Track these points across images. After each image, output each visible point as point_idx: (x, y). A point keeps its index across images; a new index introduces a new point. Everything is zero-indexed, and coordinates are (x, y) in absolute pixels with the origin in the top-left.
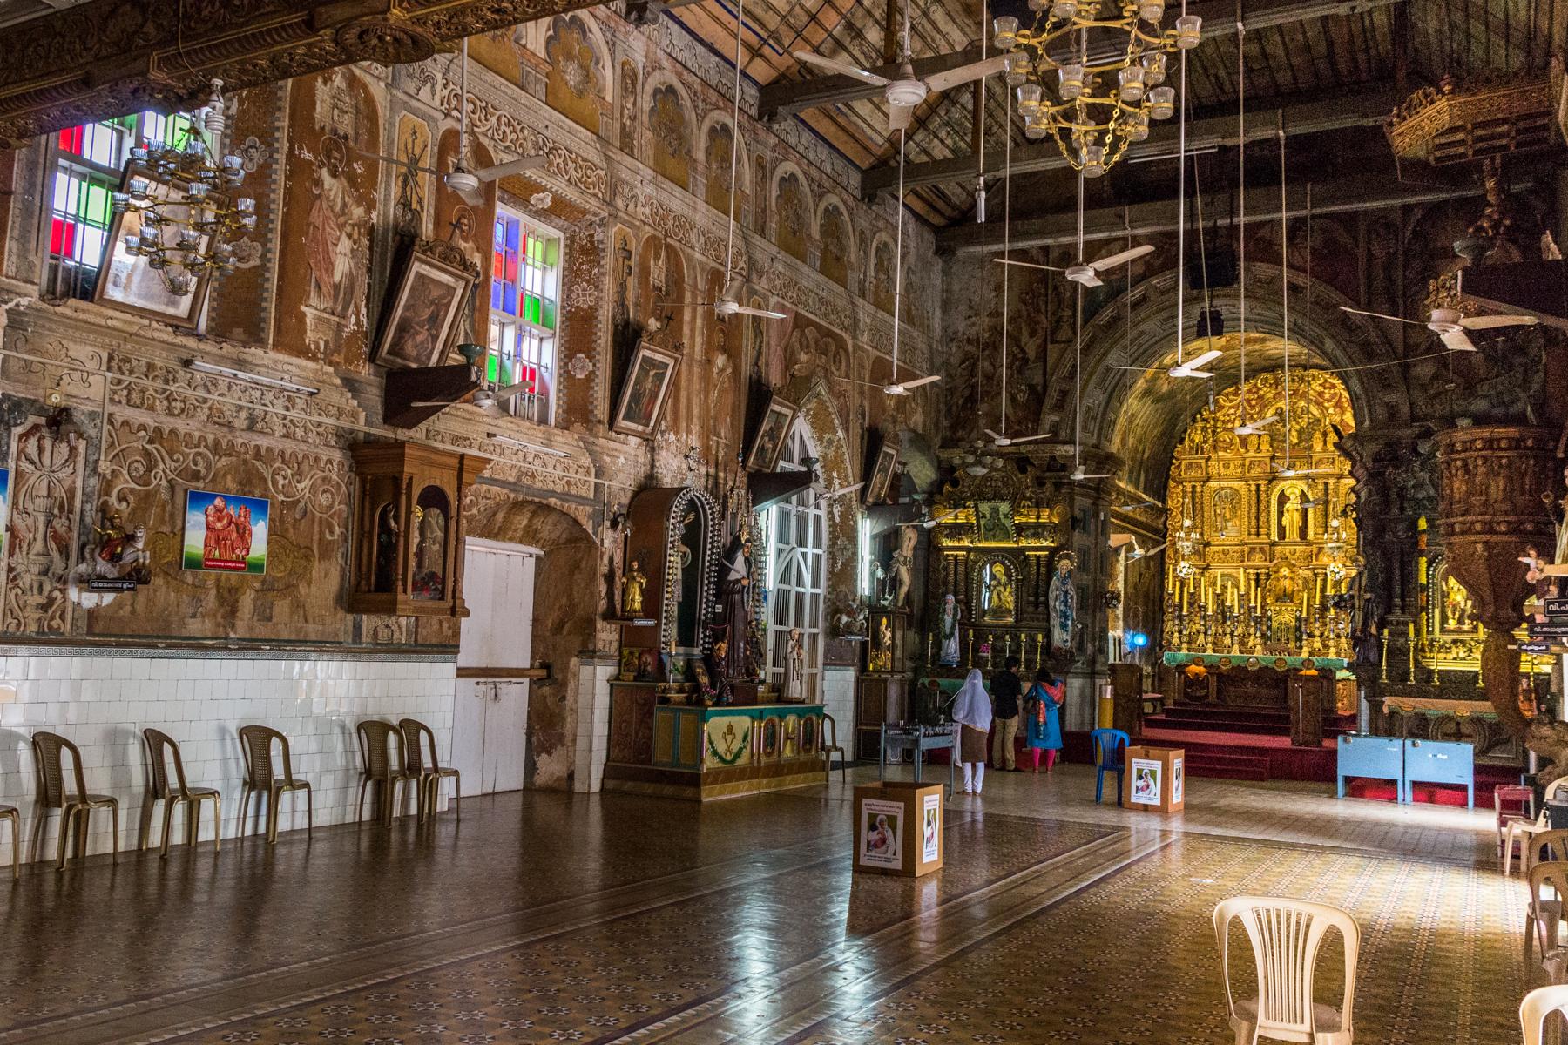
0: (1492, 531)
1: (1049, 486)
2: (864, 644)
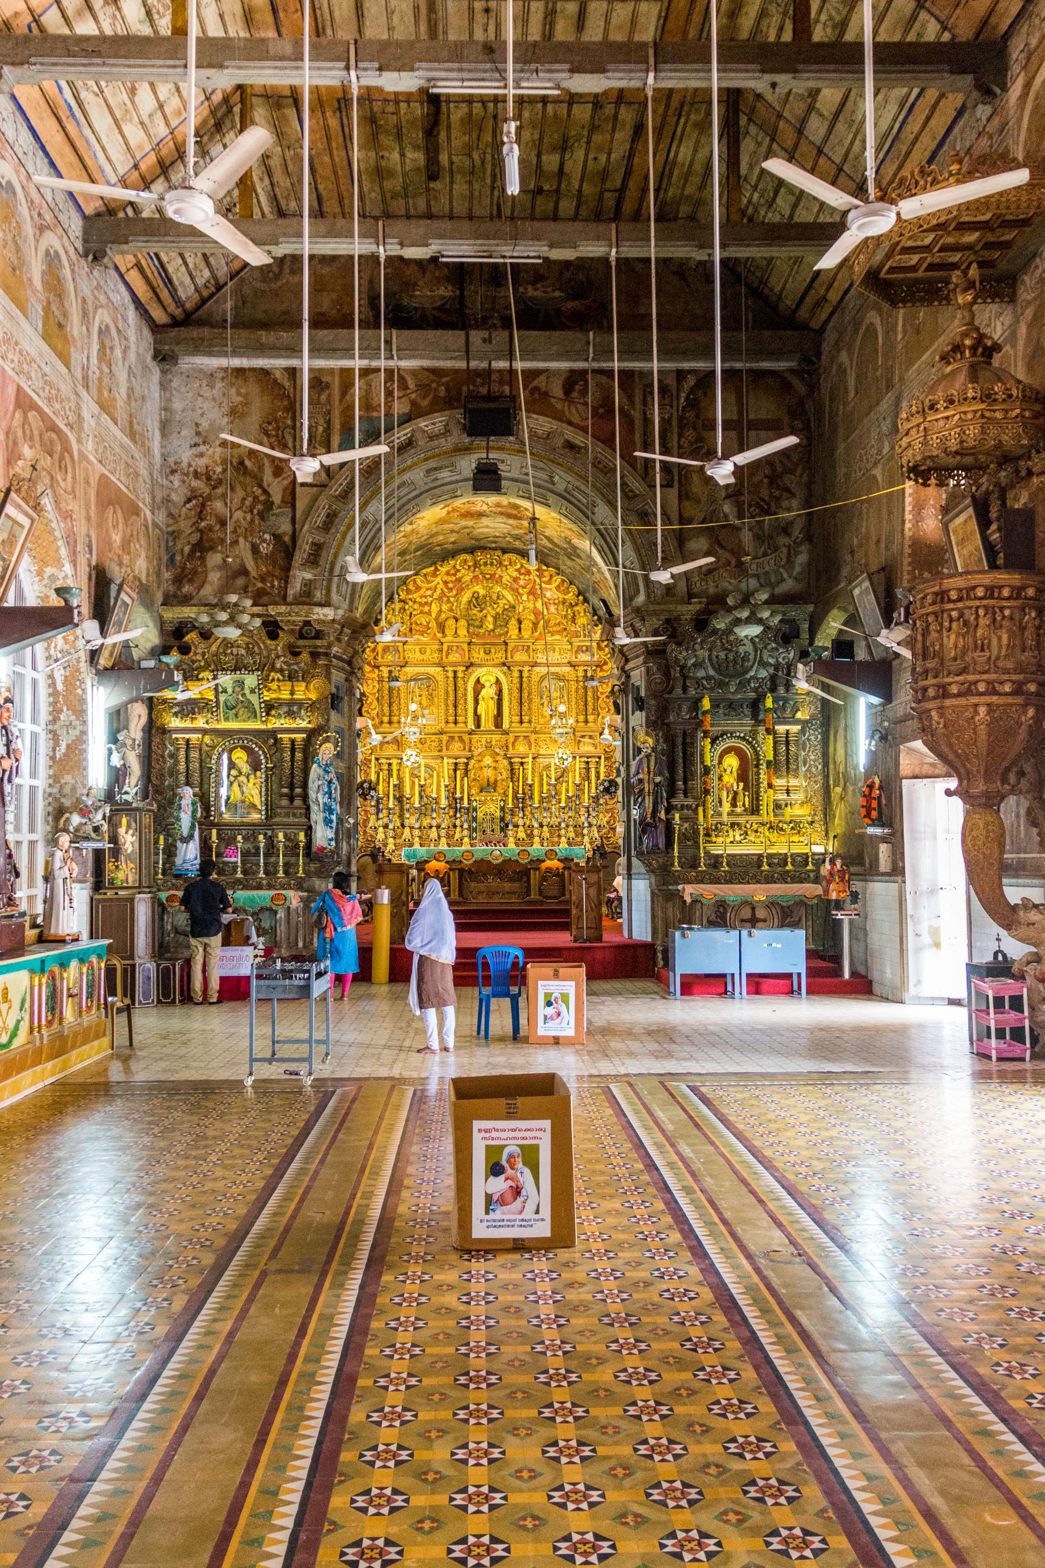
0: (995, 692)
1: (305, 656)
2: (98, 854)
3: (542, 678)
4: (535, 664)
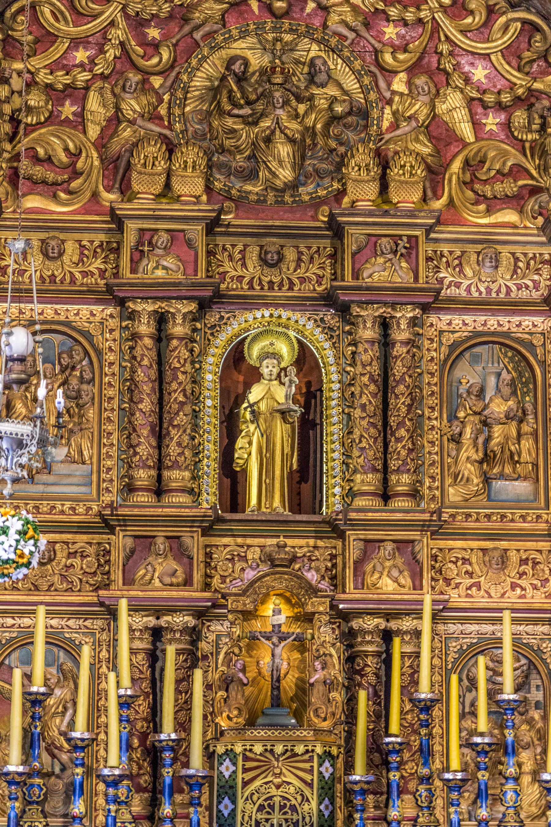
4: (433, 302)
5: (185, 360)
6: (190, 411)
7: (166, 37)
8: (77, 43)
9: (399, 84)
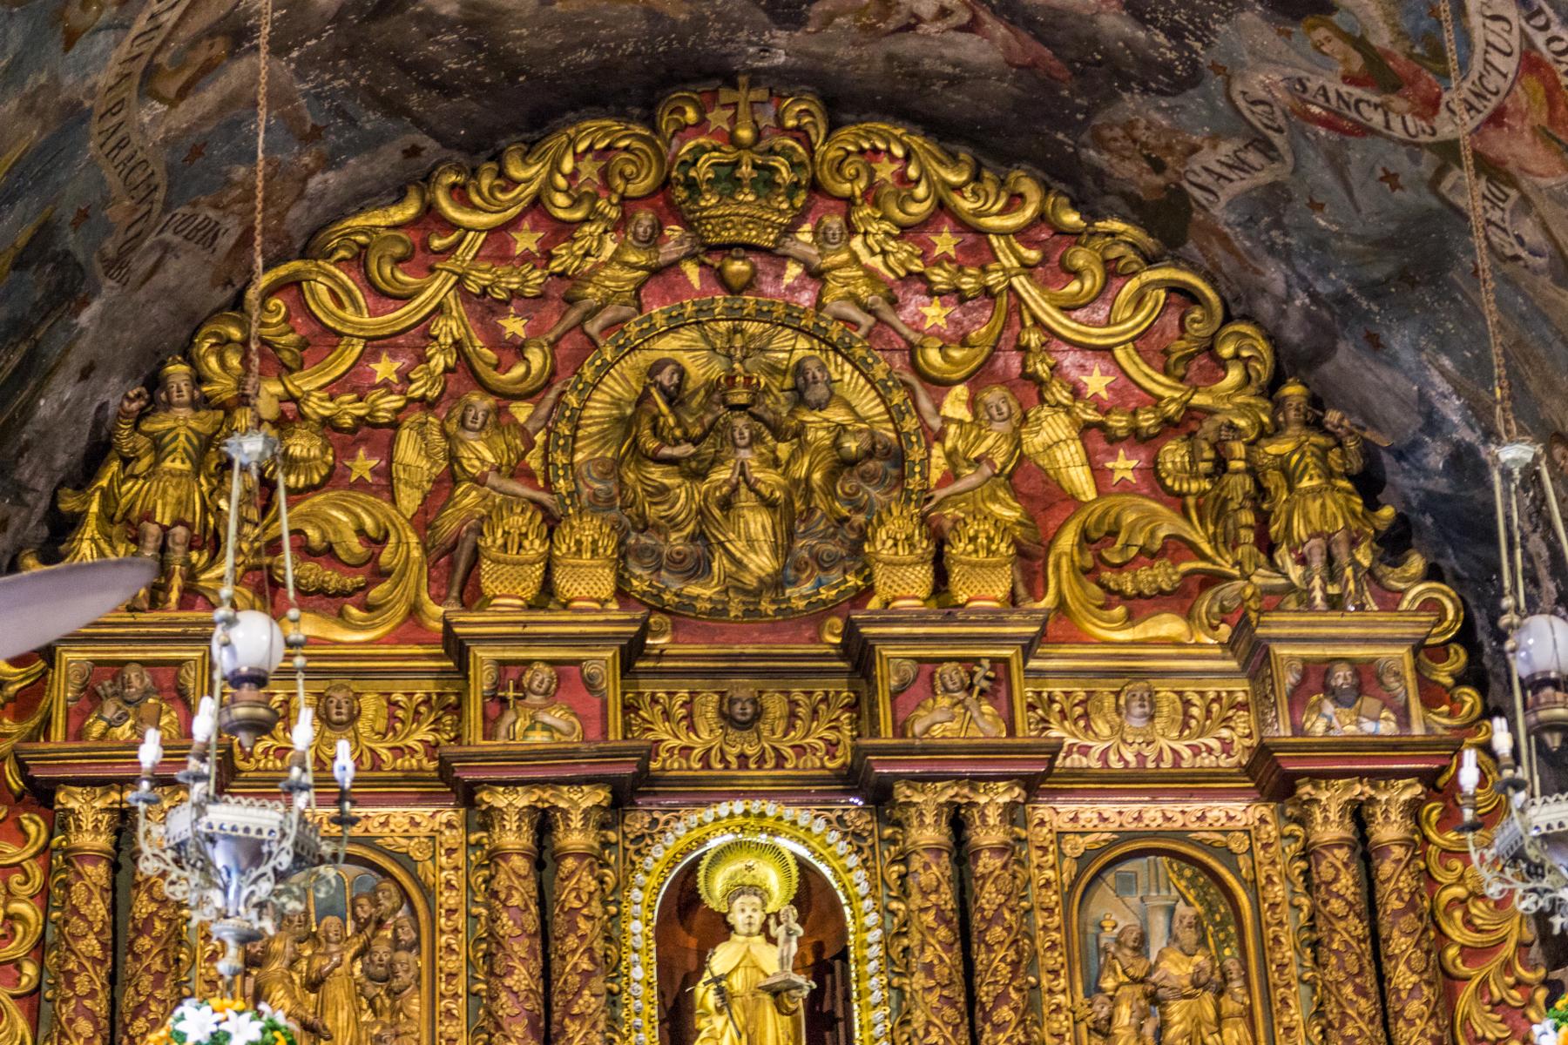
3: (1105, 863)
5: (591, 894)
6: (604, 990)
7: (535, 332)
8: (376, 345)
9: (955, 405)
